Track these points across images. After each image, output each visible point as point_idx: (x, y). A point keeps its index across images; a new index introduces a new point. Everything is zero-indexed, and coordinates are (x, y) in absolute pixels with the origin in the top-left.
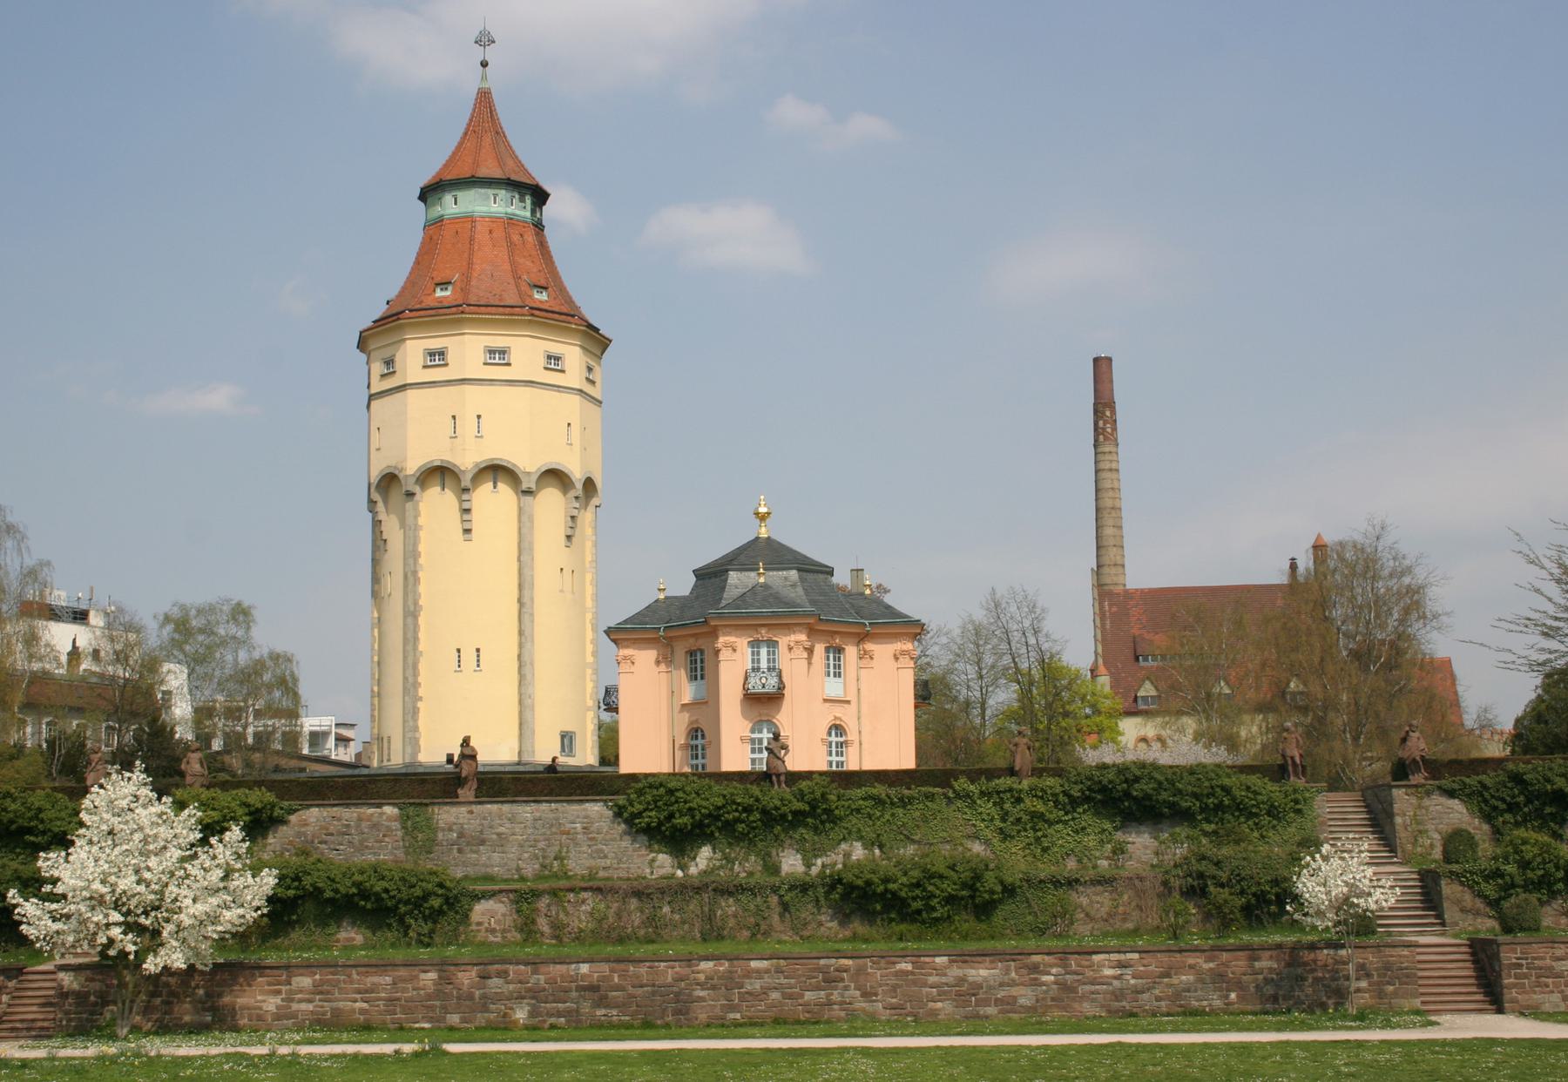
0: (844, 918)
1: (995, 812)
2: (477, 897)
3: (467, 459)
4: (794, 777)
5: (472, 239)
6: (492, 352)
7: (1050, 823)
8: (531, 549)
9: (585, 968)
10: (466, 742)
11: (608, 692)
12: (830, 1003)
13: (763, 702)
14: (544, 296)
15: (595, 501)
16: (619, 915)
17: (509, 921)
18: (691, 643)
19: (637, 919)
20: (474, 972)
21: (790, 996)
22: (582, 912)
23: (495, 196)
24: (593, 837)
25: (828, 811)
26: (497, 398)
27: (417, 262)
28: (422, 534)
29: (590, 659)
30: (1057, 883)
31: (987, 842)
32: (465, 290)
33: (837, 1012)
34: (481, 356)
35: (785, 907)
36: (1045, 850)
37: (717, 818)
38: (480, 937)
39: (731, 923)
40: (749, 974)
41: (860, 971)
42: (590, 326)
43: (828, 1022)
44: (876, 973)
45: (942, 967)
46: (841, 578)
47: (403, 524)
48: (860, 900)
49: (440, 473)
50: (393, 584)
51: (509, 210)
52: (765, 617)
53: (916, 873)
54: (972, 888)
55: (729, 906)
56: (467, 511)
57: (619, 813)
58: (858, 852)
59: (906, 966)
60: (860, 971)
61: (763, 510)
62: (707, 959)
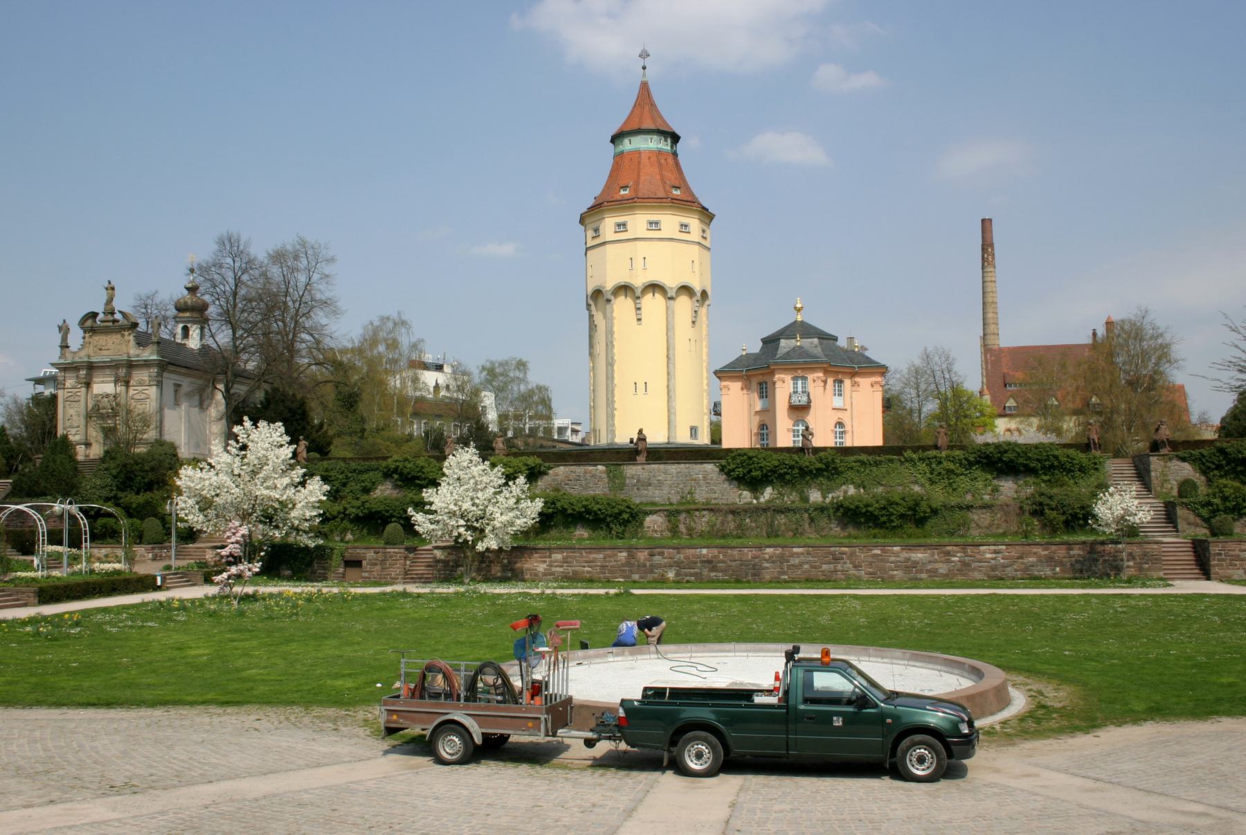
0: (844, 526)
1: (927, 469)
2: (647, 513)
3: (638, 282)
4: (817, 450)
5: (639, 163)
6: (651, 223)
7: (958, 475)
8: (673, 328)
9: (704, 551)
10: (640, 431)
11: (715, 405)
12: (836, 571)
13: (799, 410)
14: (678, 192)
15: (707, 302)
16: (722, 523)
17: (664, 526)
18: (761, 379)
19: (732, 525)
20: (646, 552)
21: (815, 567)
22: (703, 521)
24: (708, 482)
25: (835, 469)
26: (654, 247)
27: (610, 176)
29: (705, 387)
30: (961, 508)
31: (922, 485)
32: (636, 190)
33: (840, 575)
34: (645, 226)
35: (812, 520)
36: (954, 490)
37: (775, 472)
38: (649, 534)
39: (783, 528)
40: (792, 555)
41: (853, 554)
42: (703, 208)
43: (835, 581)
44: (861, 555)
45: (897, 552)
46: (842, 343)
47: (605, 317)
48: (854, 516)
49: (624, 289)
50: (600, 348)
52: (800, 364)
53: (883, 502)
54: (914, 510)
55: (781, 519)
57: (722, 469)
58: (852, 490)
59: (877, 552)
60: (853, 554)
61: (799, 306)
62: (770, 547)
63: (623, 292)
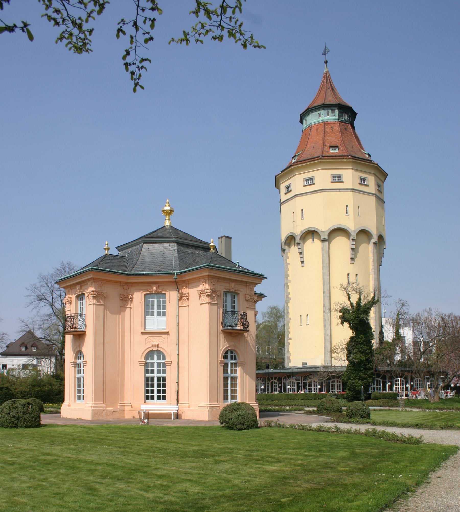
14: (336, 151)
23: (320, 114)
51: (326, 118)
61: (167, 208)
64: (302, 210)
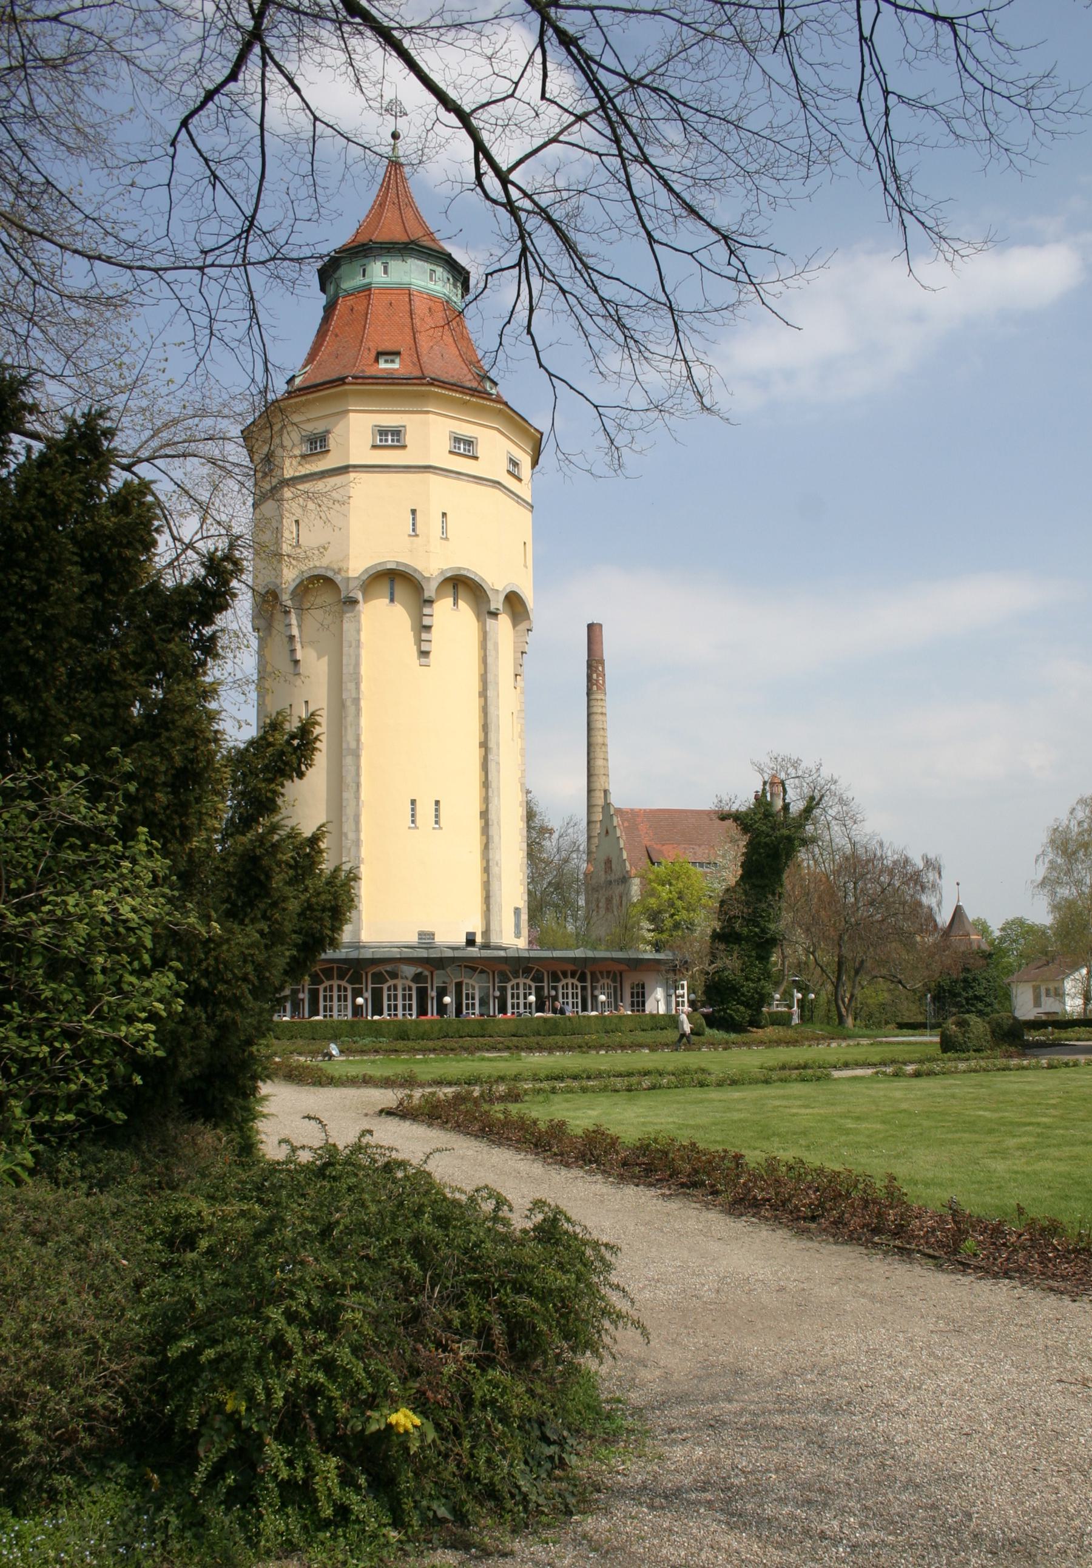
3: (432, 563)
6: (457, 440)
28: (363, 653)
34: (447, 444)
49: (394, 579)
56: (428, 628)
63: (385, 588)
64: (414, 512)
